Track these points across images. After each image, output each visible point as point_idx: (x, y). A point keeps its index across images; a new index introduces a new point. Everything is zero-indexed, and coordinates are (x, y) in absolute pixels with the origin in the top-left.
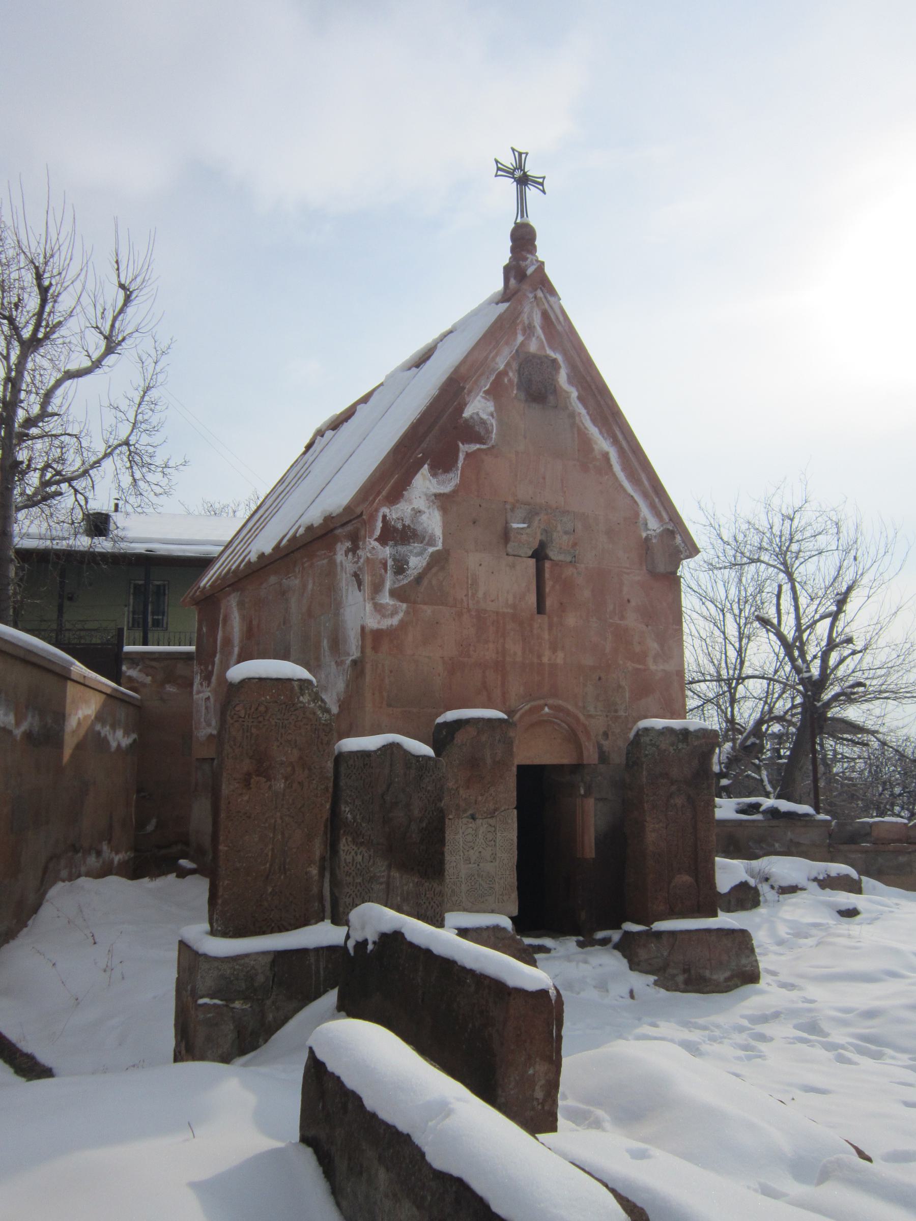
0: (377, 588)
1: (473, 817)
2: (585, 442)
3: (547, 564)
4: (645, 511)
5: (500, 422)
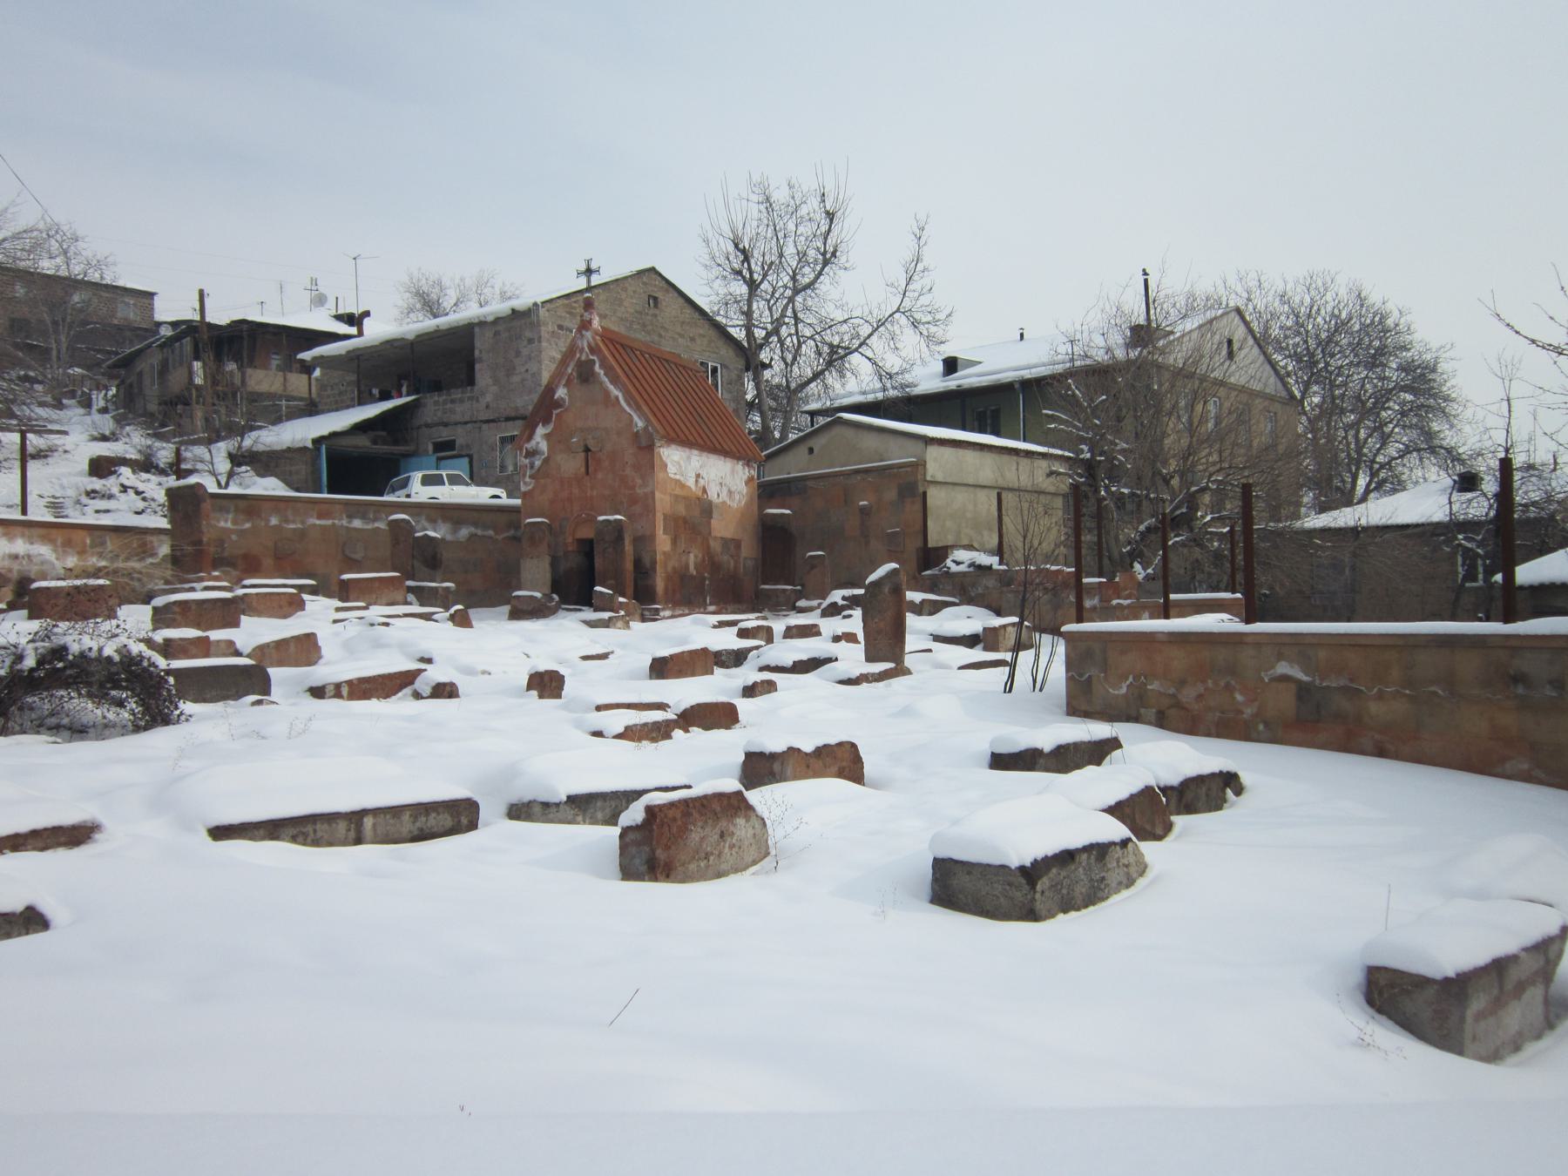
0: (524, 476)
1: (532, 558)
2: (607, 393)
3: (589, 453)
4: (636, 418)
5: (570, 397)
